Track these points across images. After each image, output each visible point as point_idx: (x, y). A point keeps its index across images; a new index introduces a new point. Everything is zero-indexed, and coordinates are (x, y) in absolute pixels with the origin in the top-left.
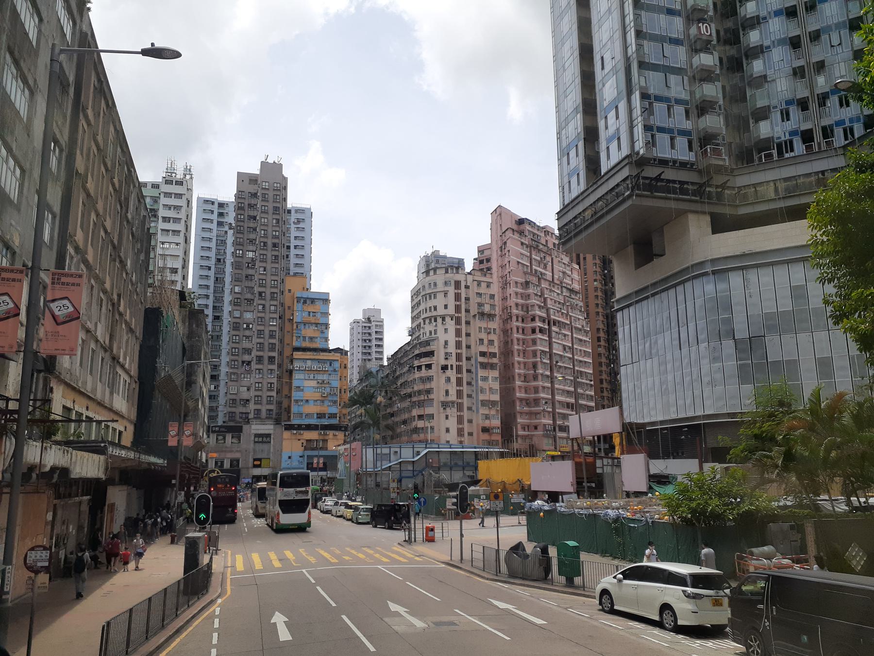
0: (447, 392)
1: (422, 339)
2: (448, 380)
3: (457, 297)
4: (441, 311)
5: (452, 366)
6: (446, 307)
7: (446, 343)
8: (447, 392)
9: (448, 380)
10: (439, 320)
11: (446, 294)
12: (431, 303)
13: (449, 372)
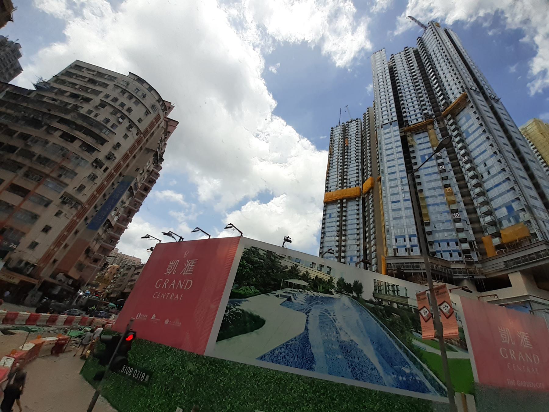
0: (81, 188)
1: (83, 111)
2: (93, 178)
3: (152, 125)
4: (134, 116)
5: (107, 169)
6: (140, 120)
7: (118, 145)
8: (81, 188)
9: (93, 178)
10: (126, 123)
11: (147, 113)
12: (129, 104)
13: (99, 172)
